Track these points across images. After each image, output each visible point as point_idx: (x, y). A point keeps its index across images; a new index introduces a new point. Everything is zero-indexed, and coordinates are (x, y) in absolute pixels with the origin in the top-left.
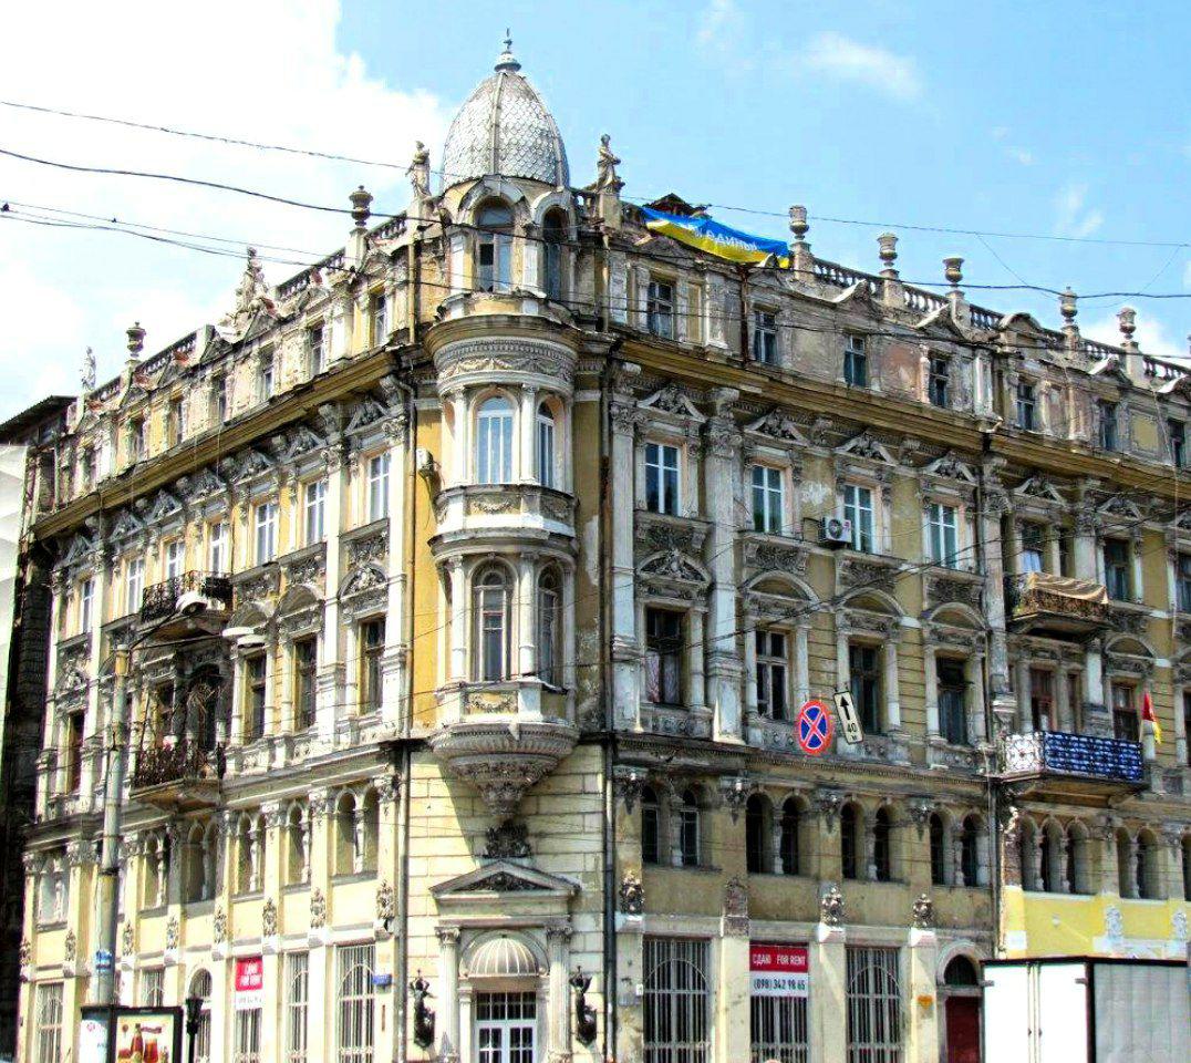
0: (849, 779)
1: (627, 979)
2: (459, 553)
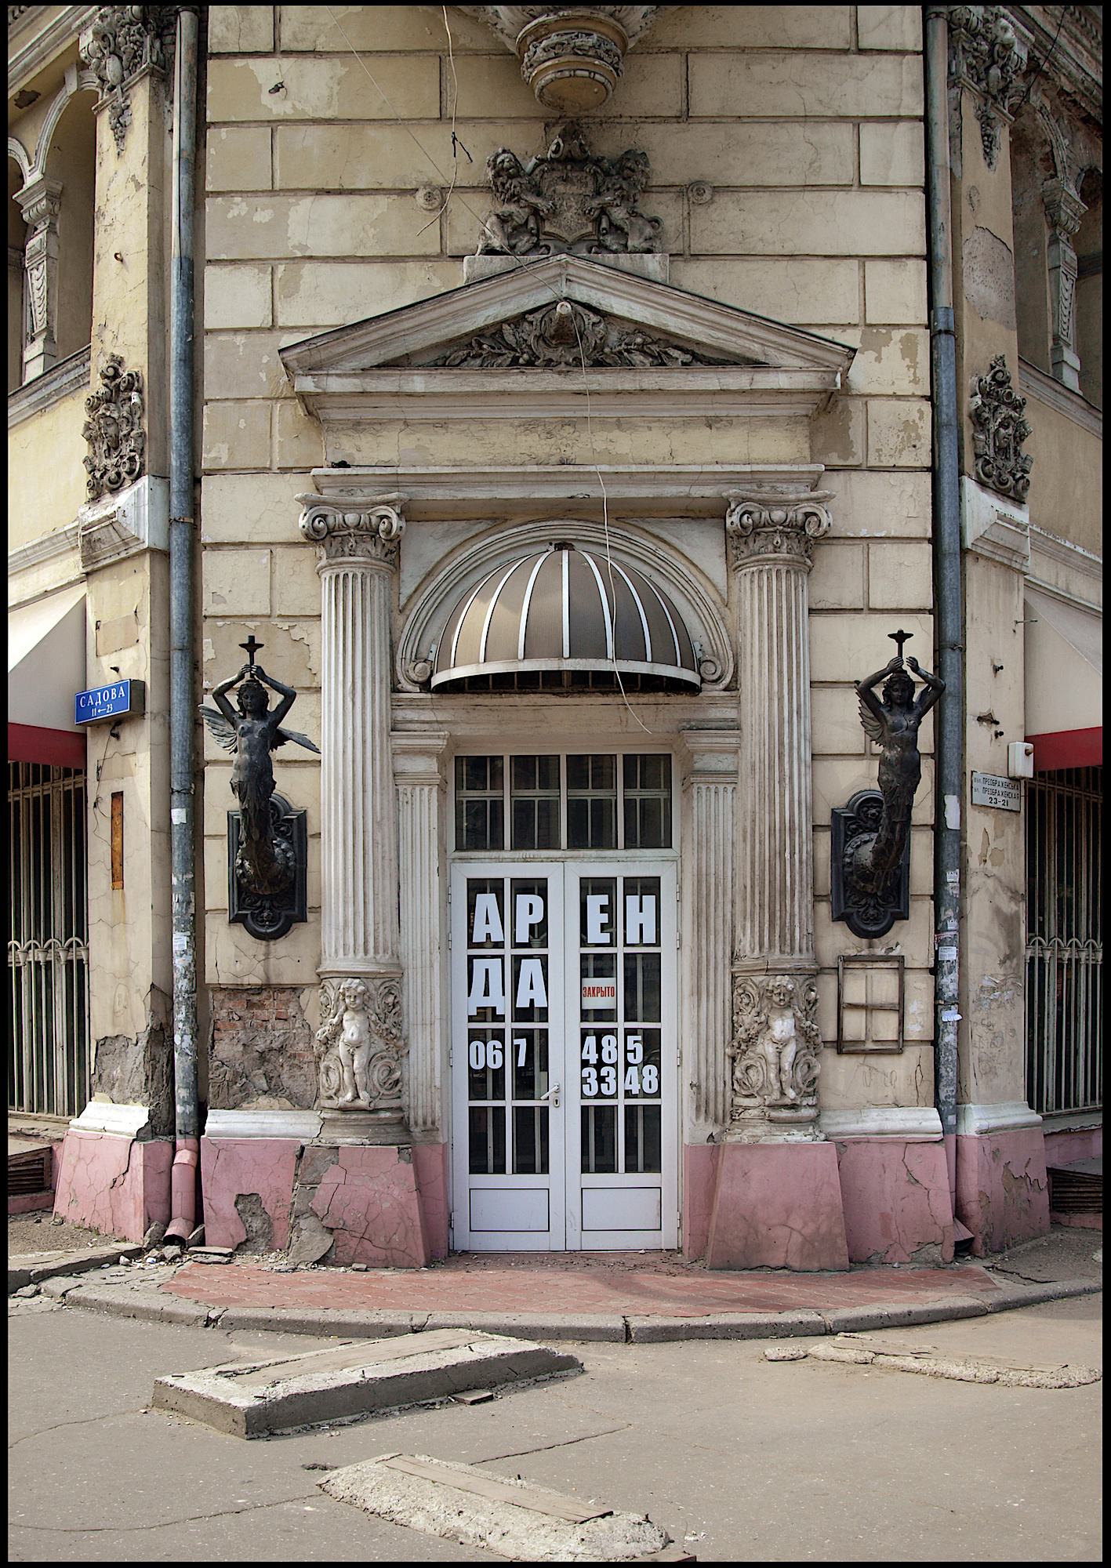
1: (988, 719)
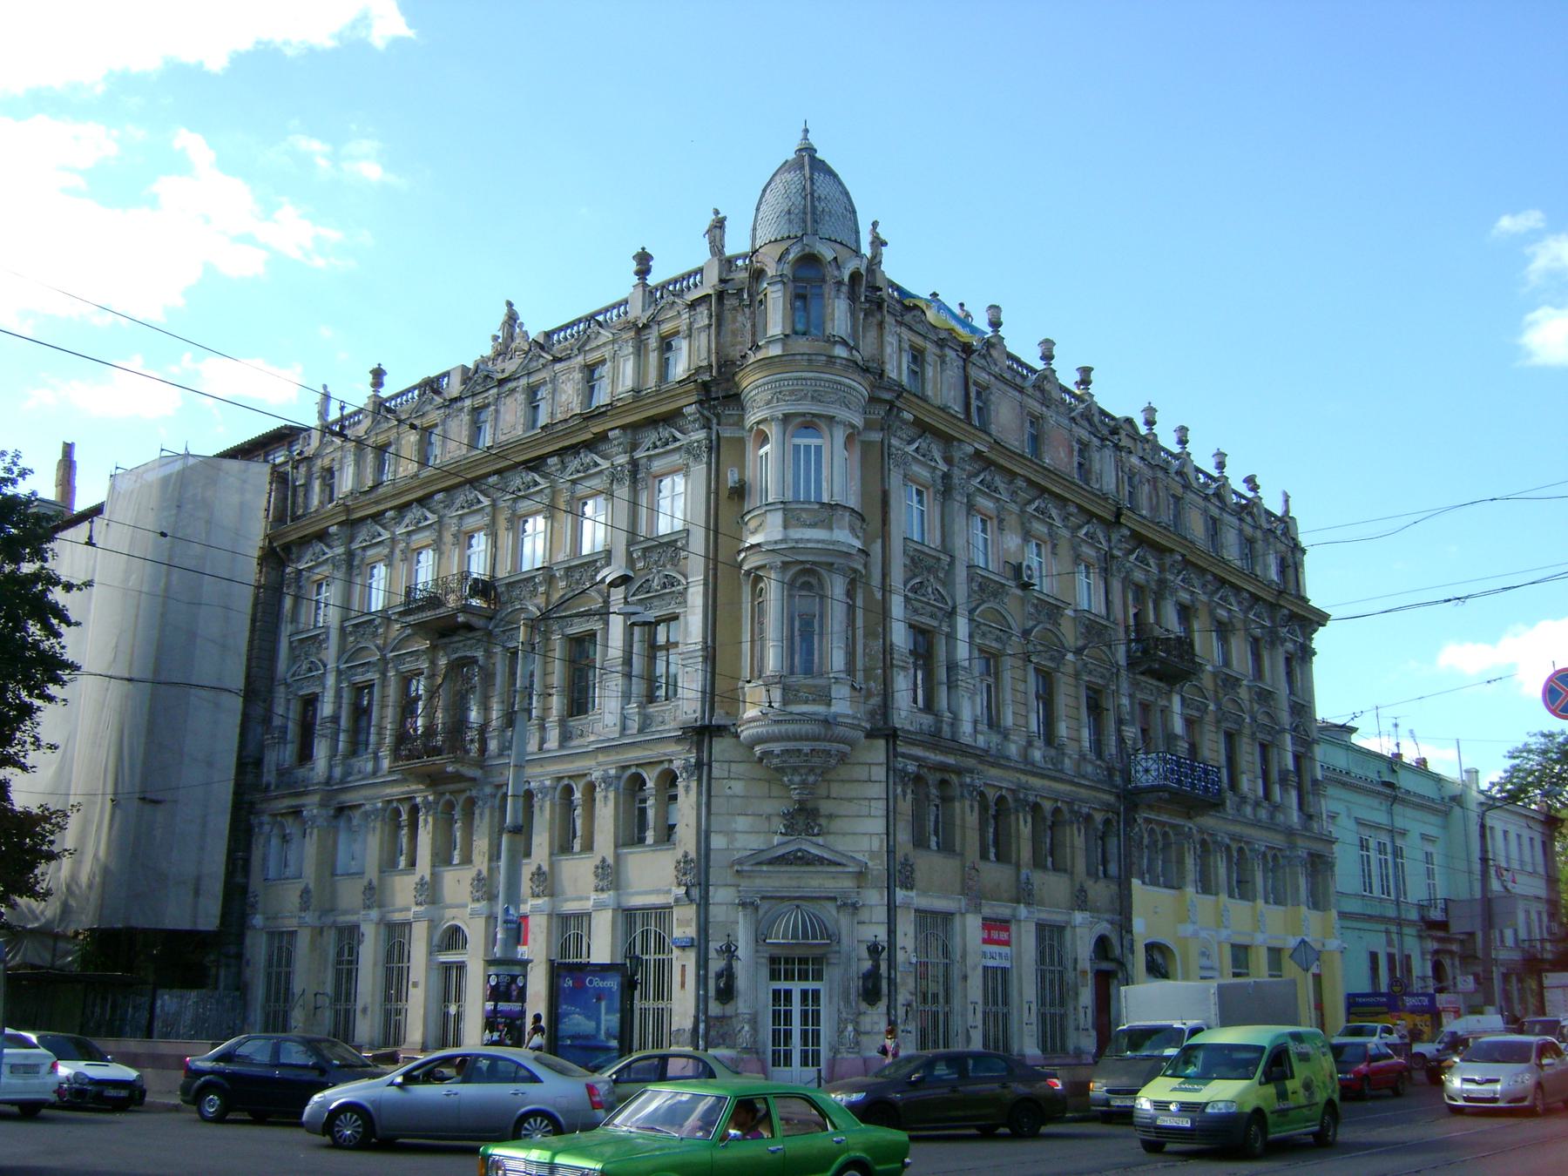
0: (1036, 782)
2: (778, 560)
